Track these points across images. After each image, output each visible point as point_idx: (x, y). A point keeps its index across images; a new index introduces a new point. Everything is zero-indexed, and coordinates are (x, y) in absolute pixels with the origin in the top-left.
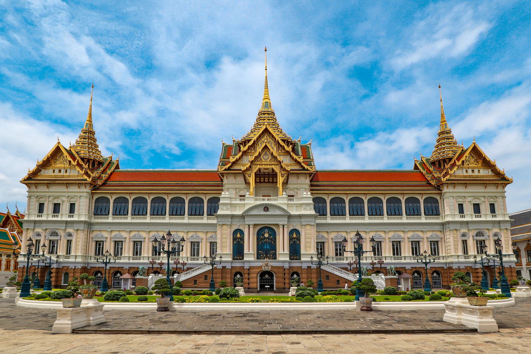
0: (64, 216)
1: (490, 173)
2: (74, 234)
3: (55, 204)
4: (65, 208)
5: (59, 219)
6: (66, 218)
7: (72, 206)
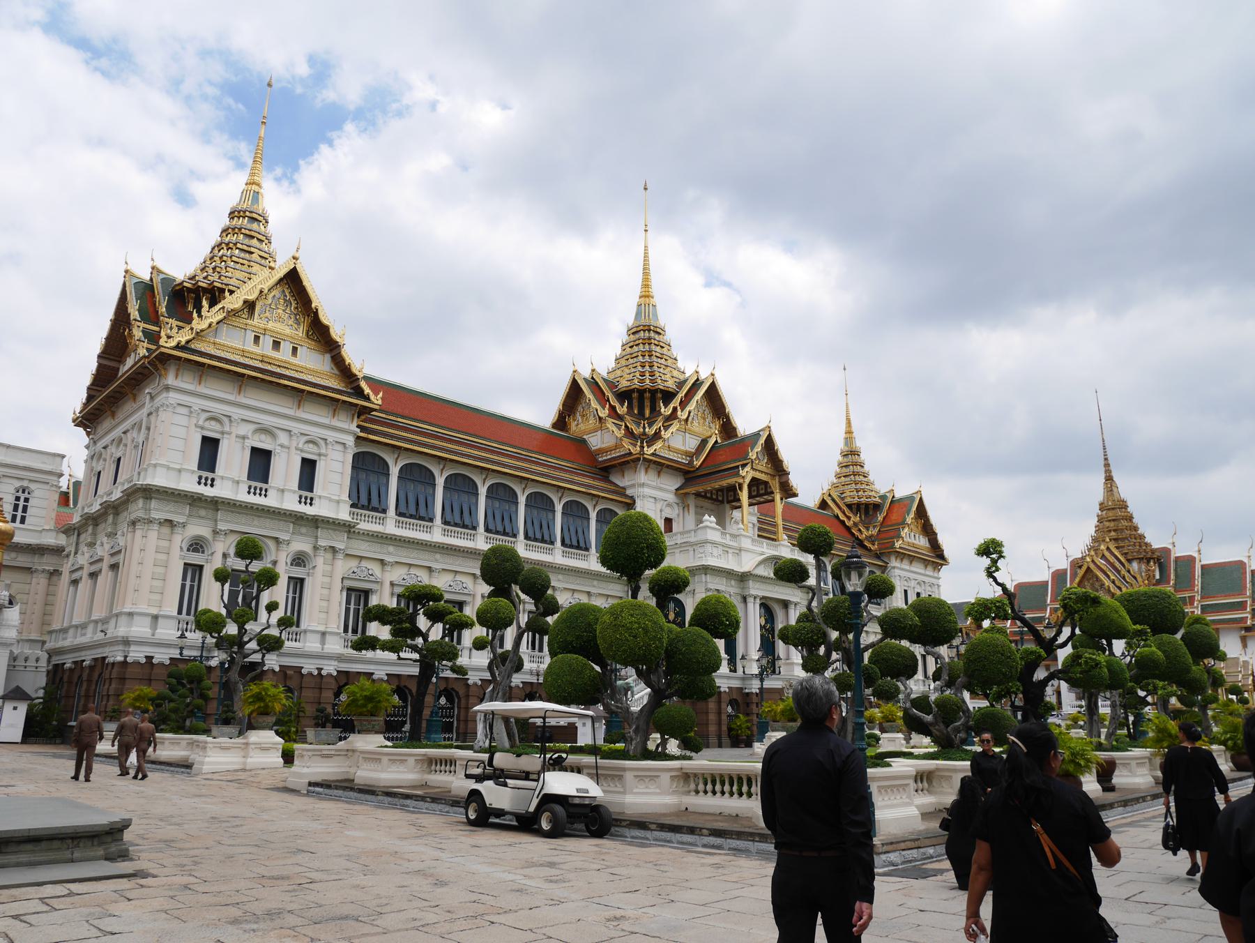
0: (282, 490)
1: (928, 545)
2: (320, 562)
3: (255, 451)
4: (285, 471)
5: (271, 501)
6: (291, 503)
7: (308, 467)
